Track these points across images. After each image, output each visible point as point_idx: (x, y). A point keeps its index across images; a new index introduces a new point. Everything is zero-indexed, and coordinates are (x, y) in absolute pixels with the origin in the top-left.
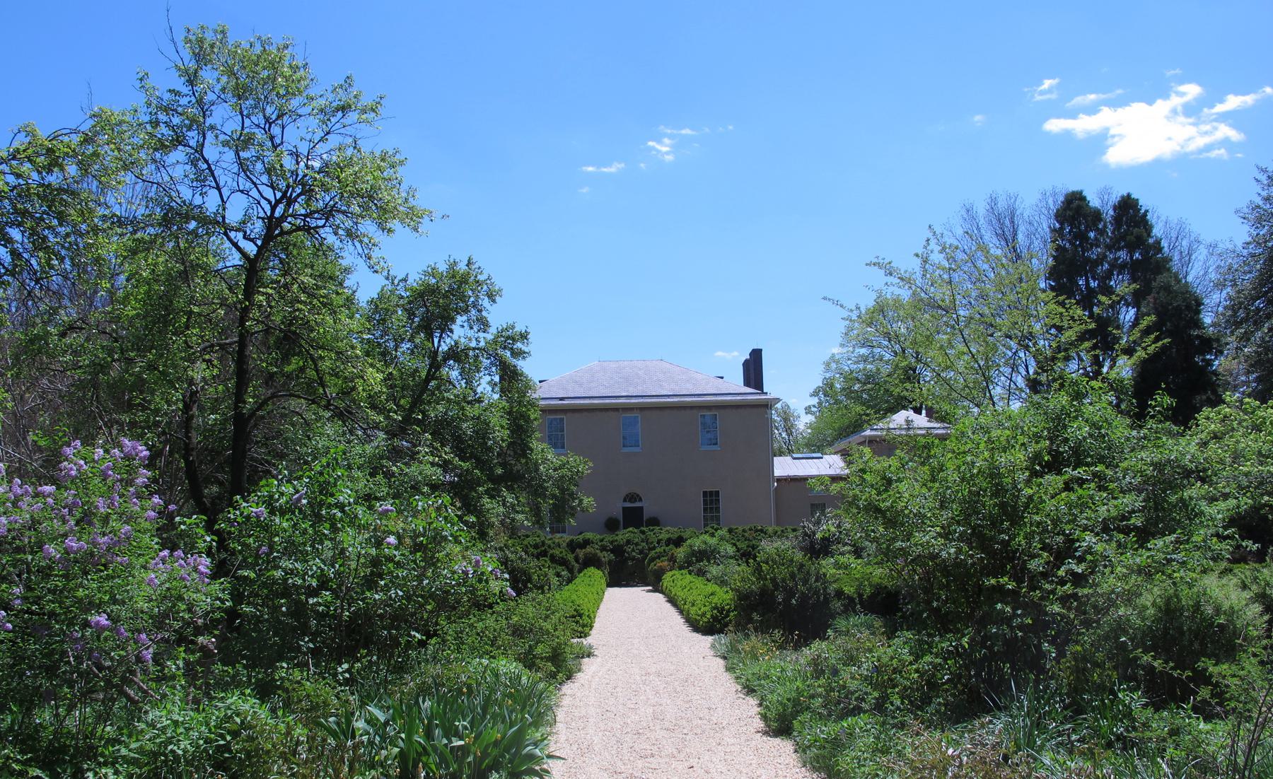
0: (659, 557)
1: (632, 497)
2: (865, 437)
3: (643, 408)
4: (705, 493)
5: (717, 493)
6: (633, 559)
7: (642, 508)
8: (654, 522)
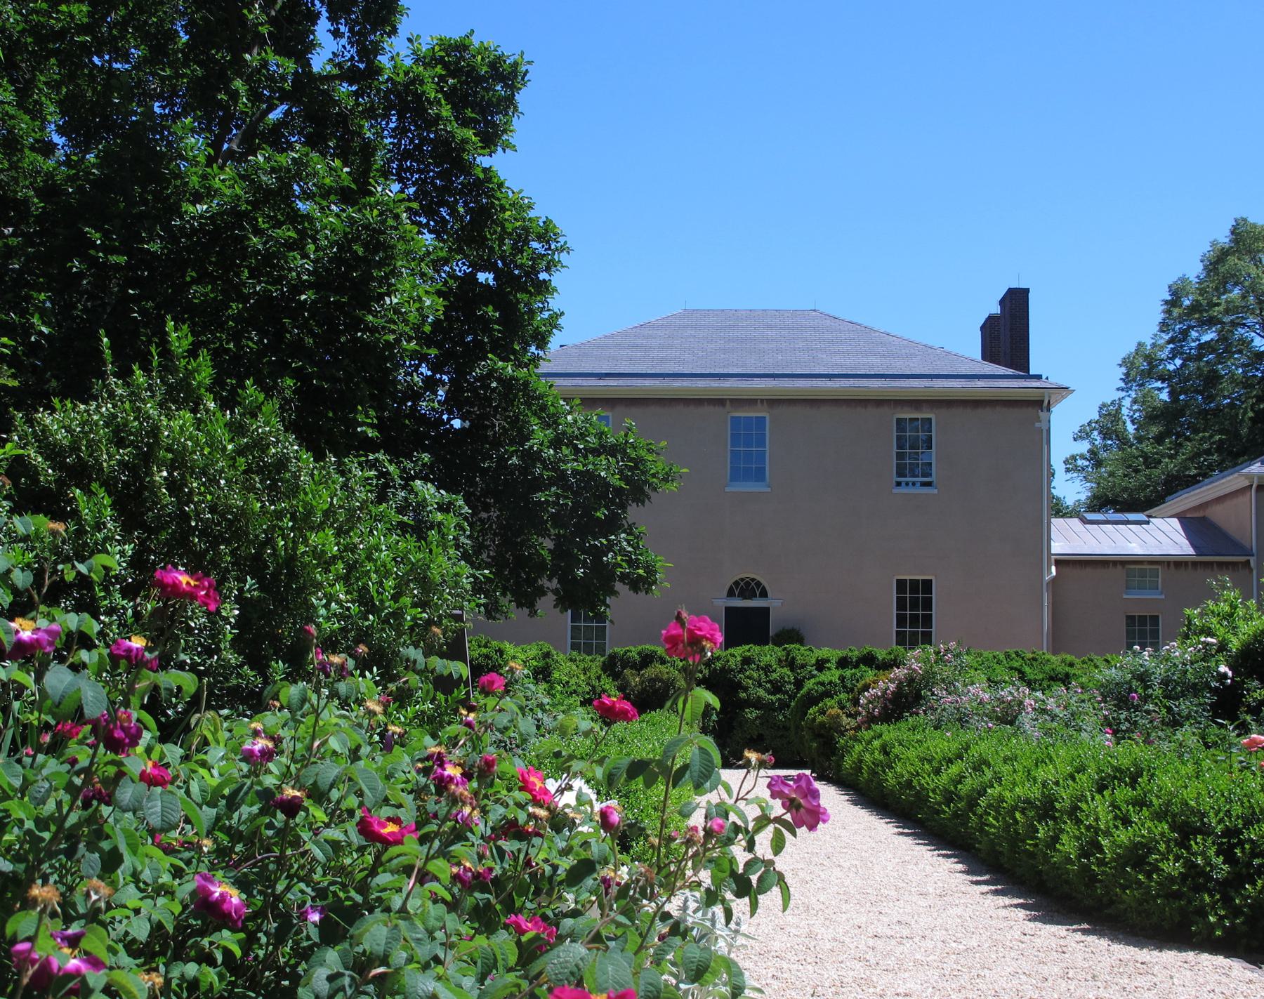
0: (828, 694)
1: (747, 588)
2: (1250, 476)
3: (774, 402)
4: (901, 585)
5: (927, 585)
6: (757, 704)
7: (768, 609)
8: (791, 636)
